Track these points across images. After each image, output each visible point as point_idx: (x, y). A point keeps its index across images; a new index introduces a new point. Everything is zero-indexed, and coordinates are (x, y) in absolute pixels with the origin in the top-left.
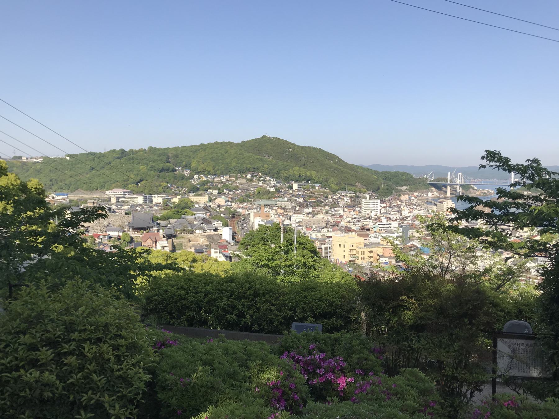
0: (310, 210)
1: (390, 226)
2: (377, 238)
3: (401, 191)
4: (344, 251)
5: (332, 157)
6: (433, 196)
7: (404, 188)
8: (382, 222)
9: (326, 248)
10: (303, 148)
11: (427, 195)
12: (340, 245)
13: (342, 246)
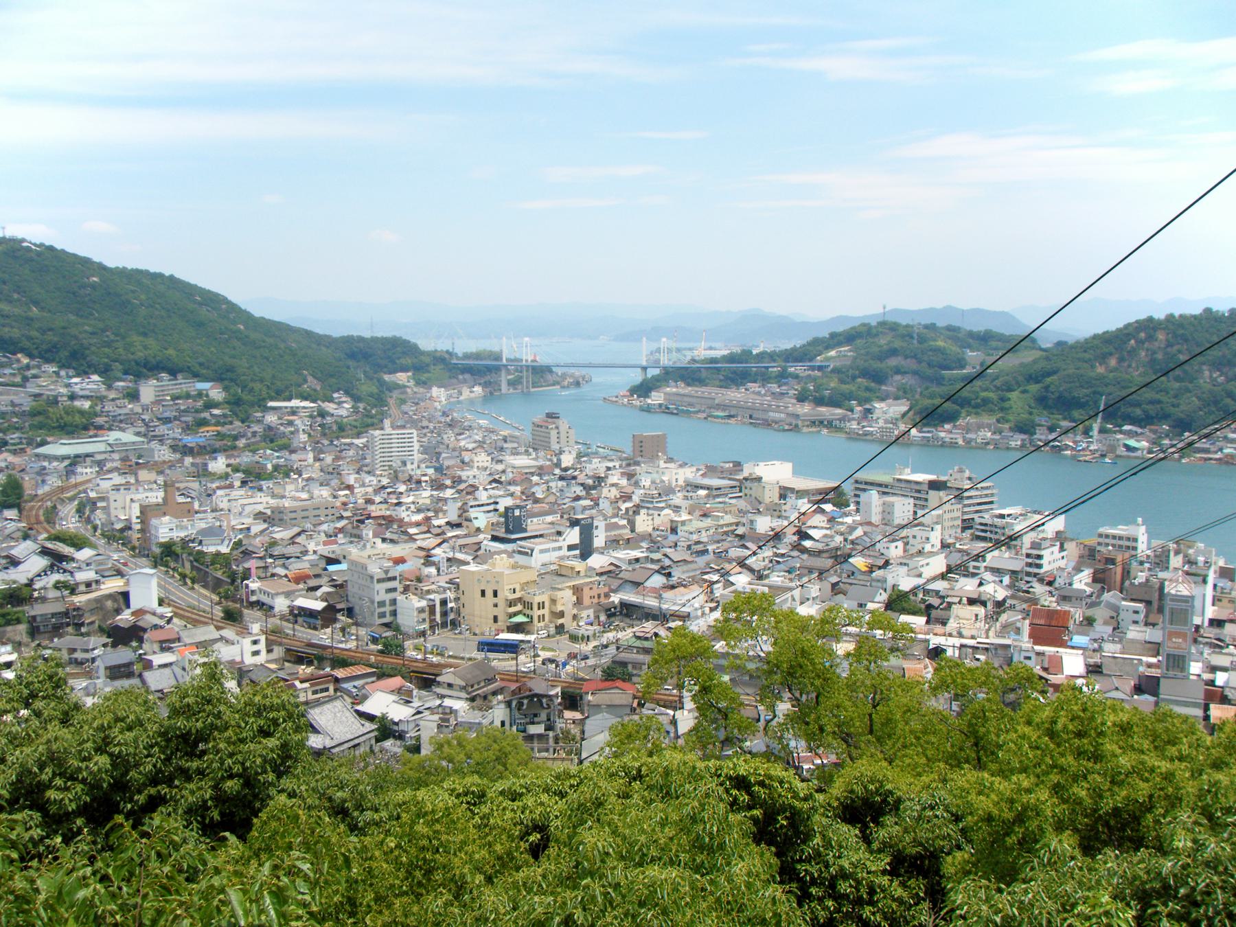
0: (219, 465)
1: (491, 508)
2: (526, 554)
3: (397, 386)
4: (496, 605)
5: (213, 300)
6: (472, 395)
7: (402, 377)
8: (476, 499)
9: (444, 602)
10: (123, 273)
11: (460, 393)
12: (483, 593)
13: (489, 593)
